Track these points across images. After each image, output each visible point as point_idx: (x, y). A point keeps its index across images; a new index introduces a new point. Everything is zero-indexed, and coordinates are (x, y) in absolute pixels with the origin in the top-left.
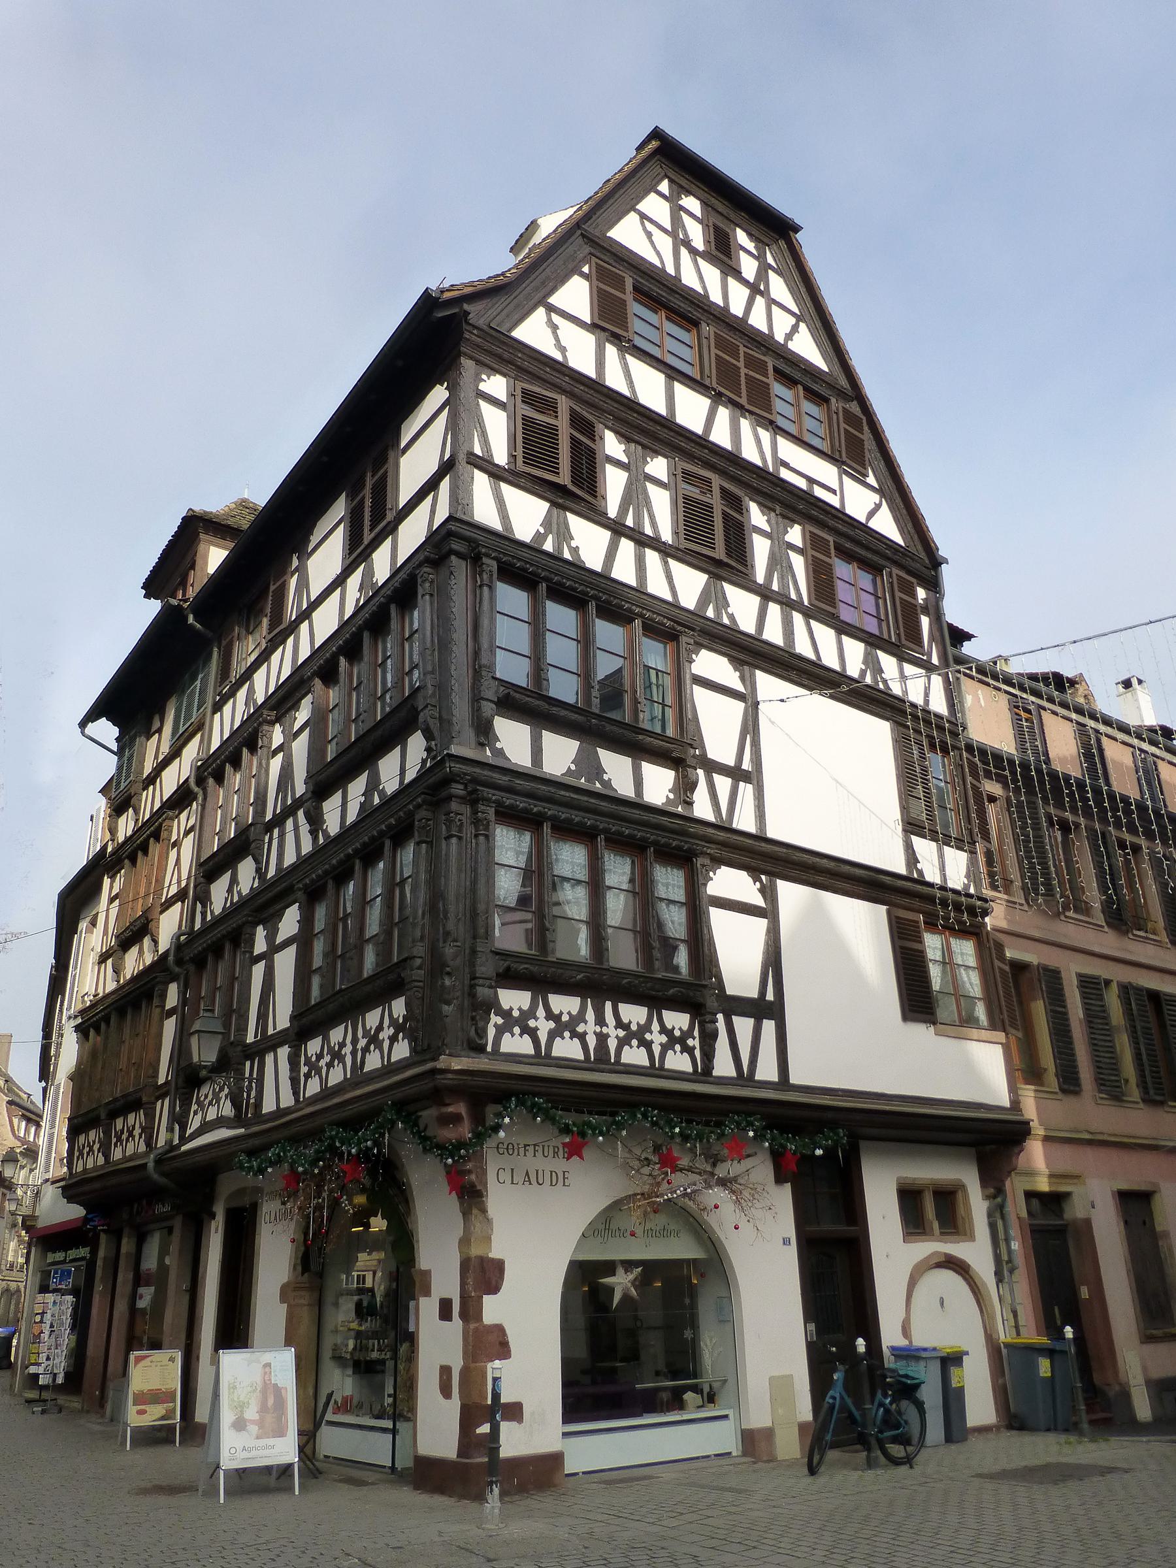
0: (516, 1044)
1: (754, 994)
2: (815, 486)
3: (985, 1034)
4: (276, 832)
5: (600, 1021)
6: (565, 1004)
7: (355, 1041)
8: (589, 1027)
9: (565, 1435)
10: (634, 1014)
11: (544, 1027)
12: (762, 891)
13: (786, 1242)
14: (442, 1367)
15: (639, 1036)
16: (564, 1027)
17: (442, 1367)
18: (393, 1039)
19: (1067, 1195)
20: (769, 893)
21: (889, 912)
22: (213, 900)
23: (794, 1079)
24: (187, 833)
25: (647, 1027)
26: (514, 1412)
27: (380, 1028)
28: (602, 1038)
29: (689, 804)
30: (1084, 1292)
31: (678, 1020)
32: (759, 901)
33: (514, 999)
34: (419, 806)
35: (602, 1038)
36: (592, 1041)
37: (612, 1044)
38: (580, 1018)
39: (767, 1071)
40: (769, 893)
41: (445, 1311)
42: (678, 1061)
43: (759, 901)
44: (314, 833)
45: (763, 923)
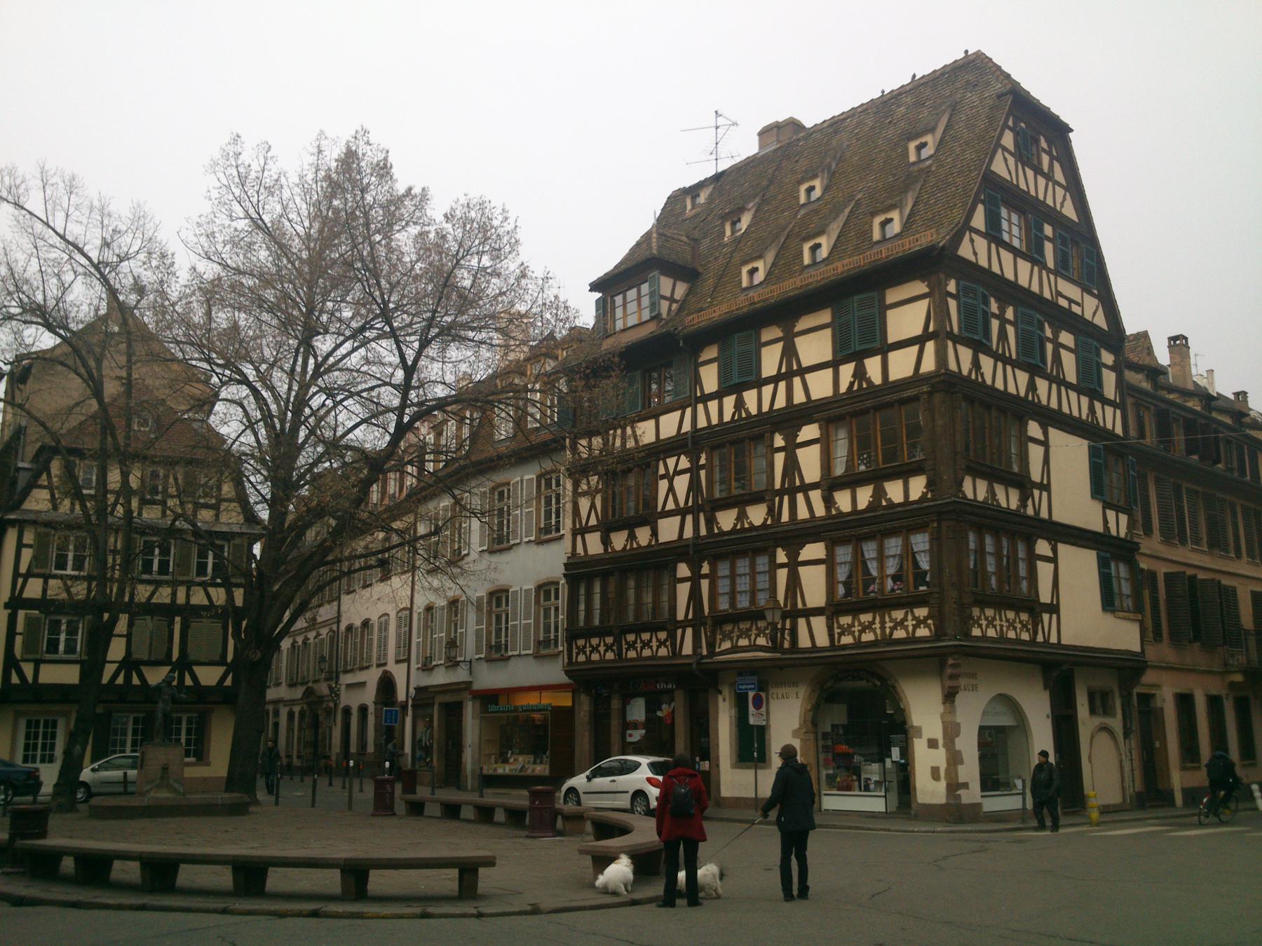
0: (976, 632)
1: (1049, 602)
2: (1073, 305)
3: (1131, 616)
4: (786, 498)
5: (1001, 620)
6: (990, 612)
7: (883, 623)
8: (997, 622)
9: (982, 796)
10: (1011, 615)
11: (984, 623)
12: (1052, 549)
13: (1048, 717)
14: (932, 768)
15: (1011, 625)
16: (991, 623)
17: (932, 768)
18: (915, 627)
19: (1154, 695)
20: (1055, 550)
21: (1098, 554)
22: (719, 521)
23: (1063, 642)
24: (678, 473)
25: (1014, 621)
26: (965, 786)
27: (905, 619)
28: (1002, 626)
29: (1025, 506)
30: (1157, 744)
31: (1024, 617)
32: (1050, 554)
33: (976, 612)
34: (933, 521)
35: (1002, 626)
36: (998, 628)
37: (1005, 629)
38: (994, 619)
39: (1054, 639)
40: (1055, 550)
41: (932, 744)
42: (1025, 636)
43: (1050, 554)
44: (828, 508)
45: (1052, 565)
